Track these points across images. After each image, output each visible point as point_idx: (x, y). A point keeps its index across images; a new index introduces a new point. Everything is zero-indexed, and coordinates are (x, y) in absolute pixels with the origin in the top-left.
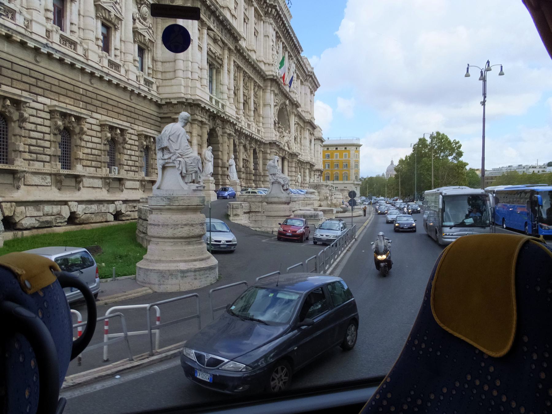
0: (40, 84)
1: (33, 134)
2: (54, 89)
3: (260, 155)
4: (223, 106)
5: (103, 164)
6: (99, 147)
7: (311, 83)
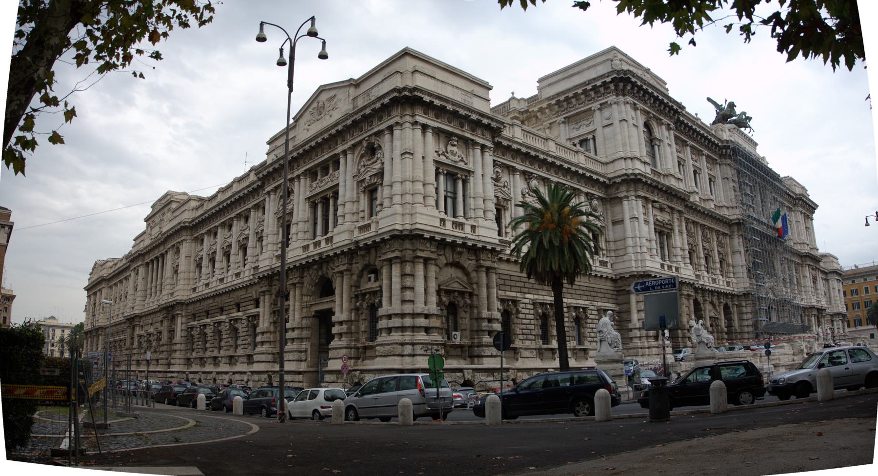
0: (527, 285)
3: (734, 310)
4: (677, 269)
7: (804, 208)
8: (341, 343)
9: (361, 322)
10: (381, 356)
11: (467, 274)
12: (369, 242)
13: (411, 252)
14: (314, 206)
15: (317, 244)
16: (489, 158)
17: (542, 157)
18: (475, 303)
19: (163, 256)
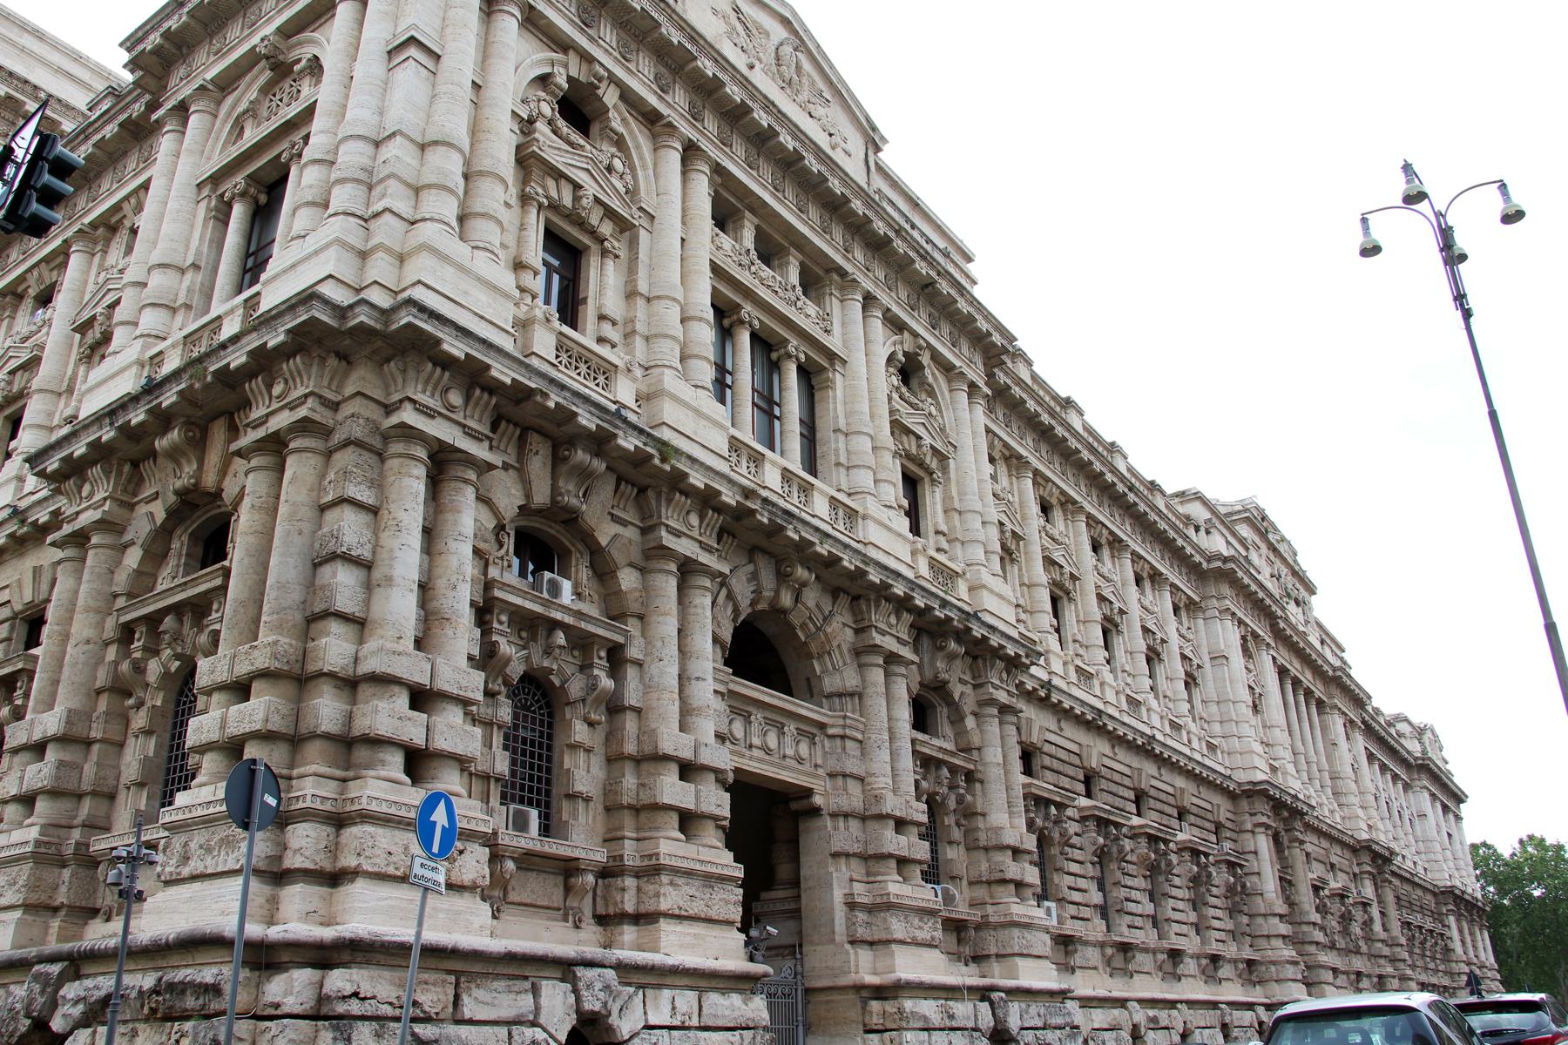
9: (131, 741)
13: (374, 412)
18: (632, 697)
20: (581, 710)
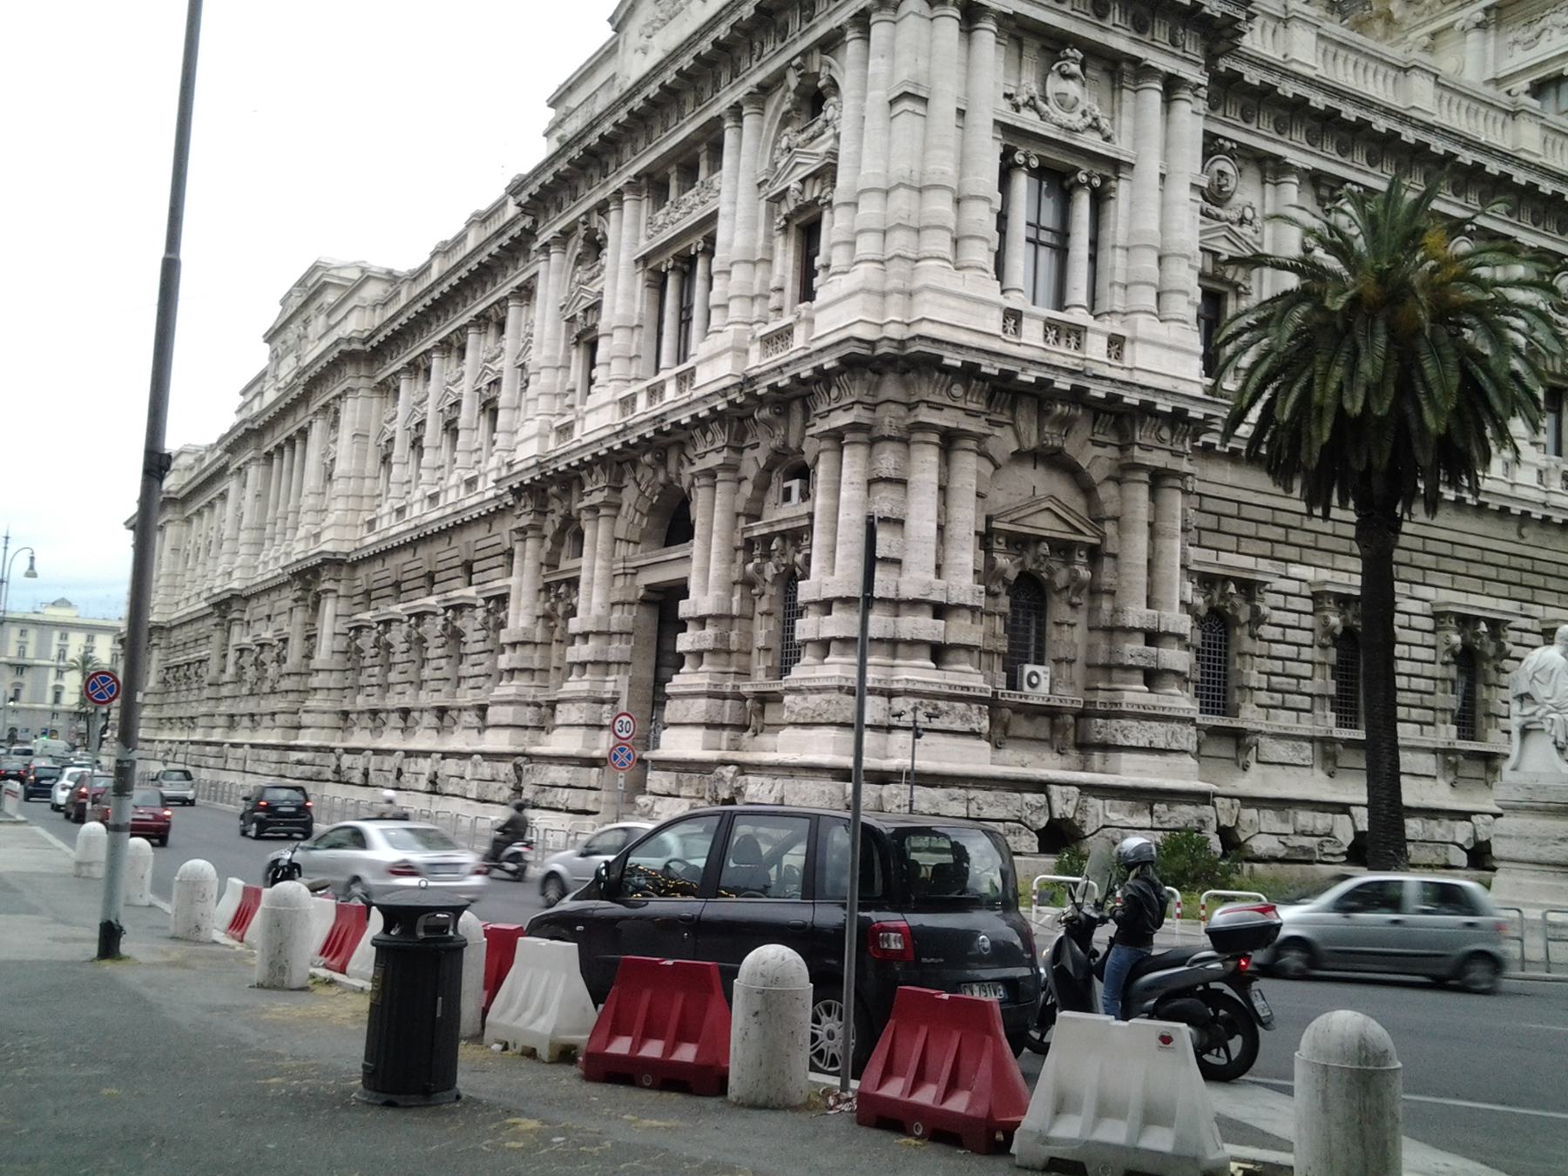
0: (1295, 537)
1: (1279, 650)
2: (1324, 542)
5: (1440, 715)
6: (1428, 670)
8: (696, 679)
10: (795, 724)
11: (1087, 489)
12: (783, 381)
13: (902, 411)
14: (658, 283)
15: (655, 392)
16: (1191, 120)
17: (1381, 124)
18: (1107, 579)
19: (303, 433)
20: (1065, 595)
